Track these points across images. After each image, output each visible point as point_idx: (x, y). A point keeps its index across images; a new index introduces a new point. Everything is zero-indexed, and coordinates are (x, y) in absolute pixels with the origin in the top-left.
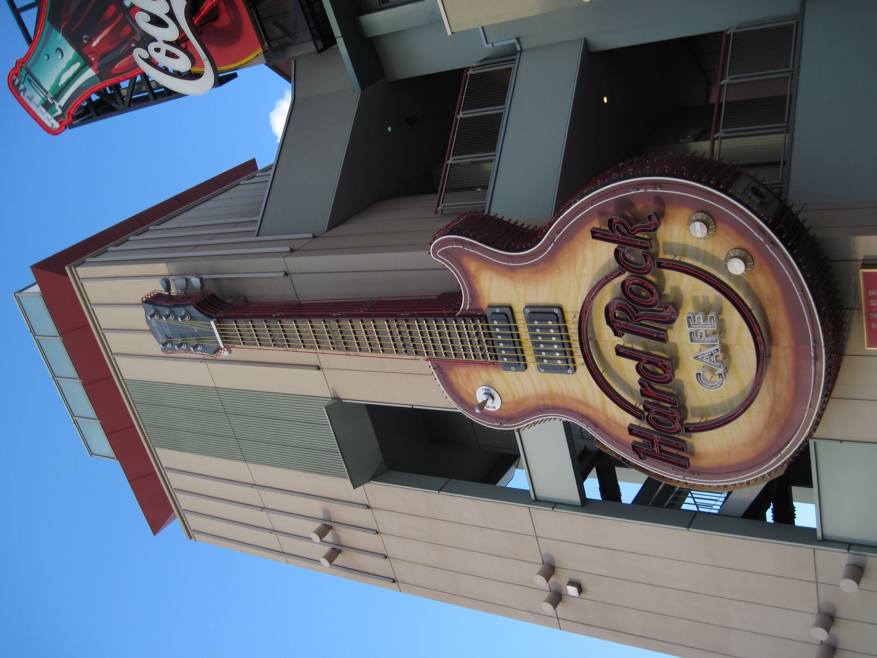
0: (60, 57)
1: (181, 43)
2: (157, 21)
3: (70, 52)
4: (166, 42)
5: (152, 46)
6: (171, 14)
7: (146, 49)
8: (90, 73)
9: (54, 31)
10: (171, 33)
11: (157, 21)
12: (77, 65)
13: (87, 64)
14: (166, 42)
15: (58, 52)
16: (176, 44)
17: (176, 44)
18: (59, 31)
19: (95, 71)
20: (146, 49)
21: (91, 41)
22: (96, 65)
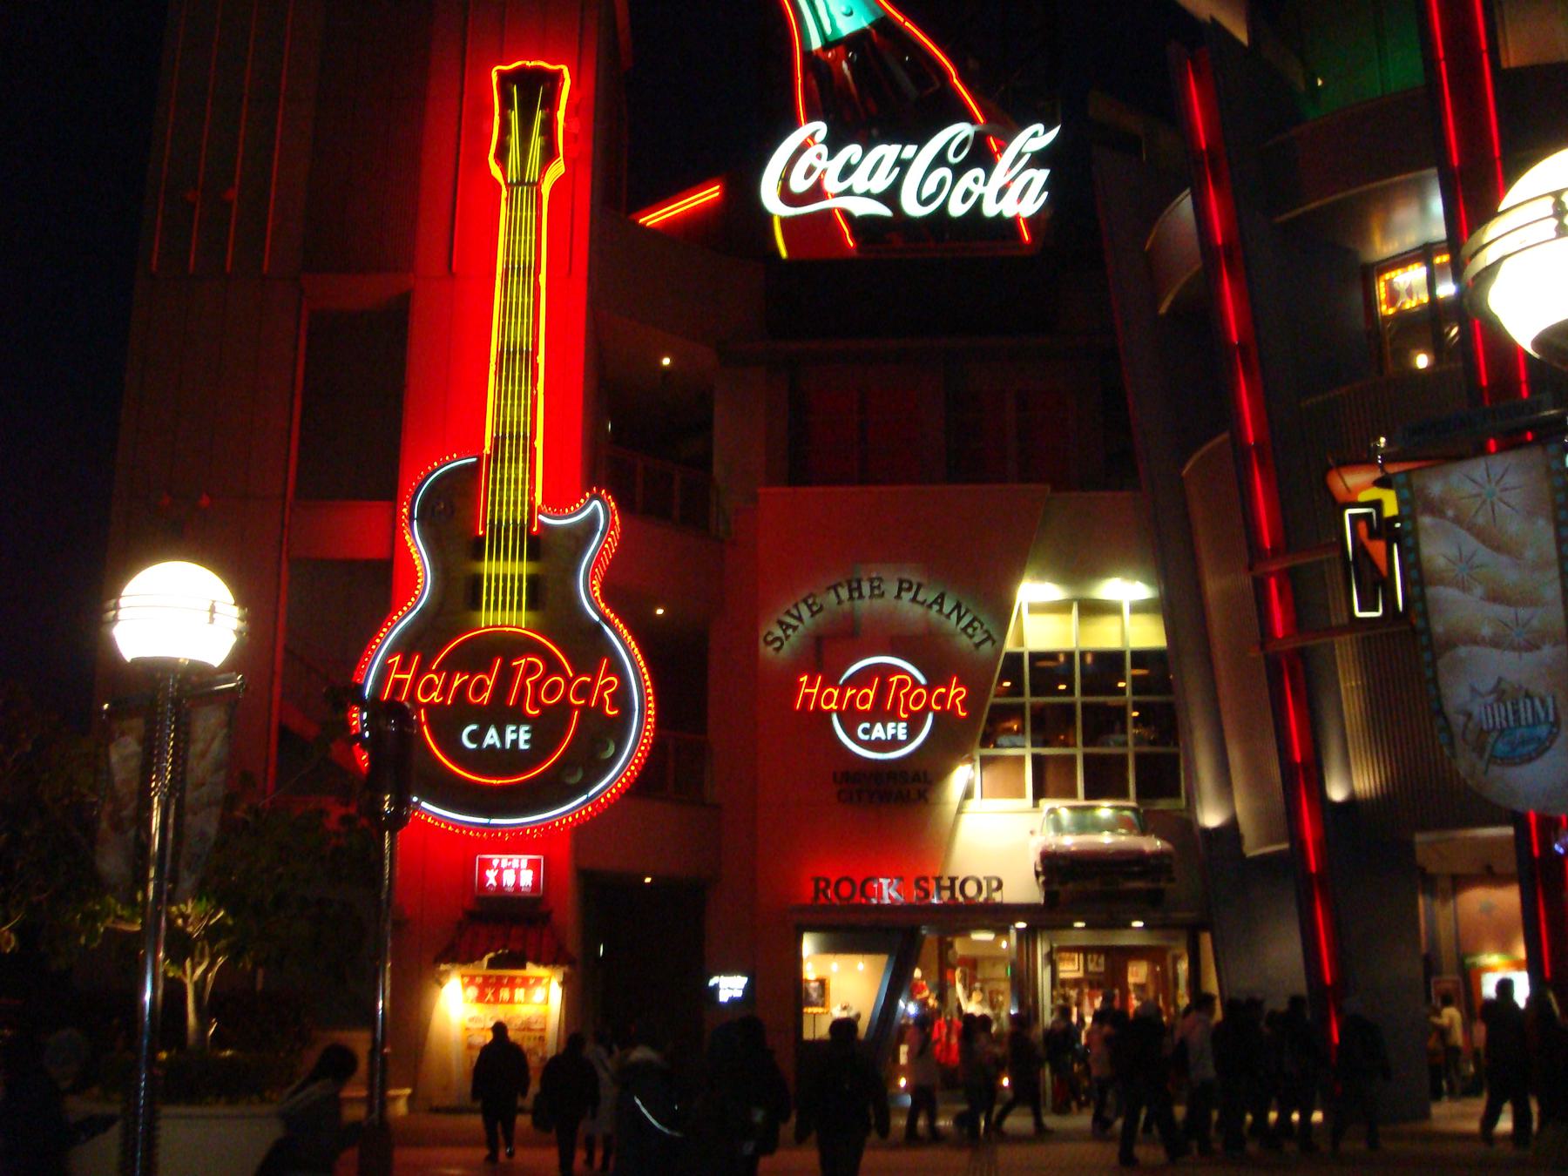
0: (844, 10)
1: (817, 193)
2: (848, 171)
3: (847, 27)
4: (824, 171)
5: (824, 150)
6: (849, 192)
7: (823, 142)
8: (816, 43)
9: (872, 19)
10: (832, 185)
11: (848, 171)
12: (828, 31)
13: (828, 45)
14: (824, 171)
15: (849, 11)
16: (819, 182)
17: (819, 182)
18: (872, 24)
19: (816, 51)
20: (823, 142)
21: (849, 62)
22: (820, 54)
